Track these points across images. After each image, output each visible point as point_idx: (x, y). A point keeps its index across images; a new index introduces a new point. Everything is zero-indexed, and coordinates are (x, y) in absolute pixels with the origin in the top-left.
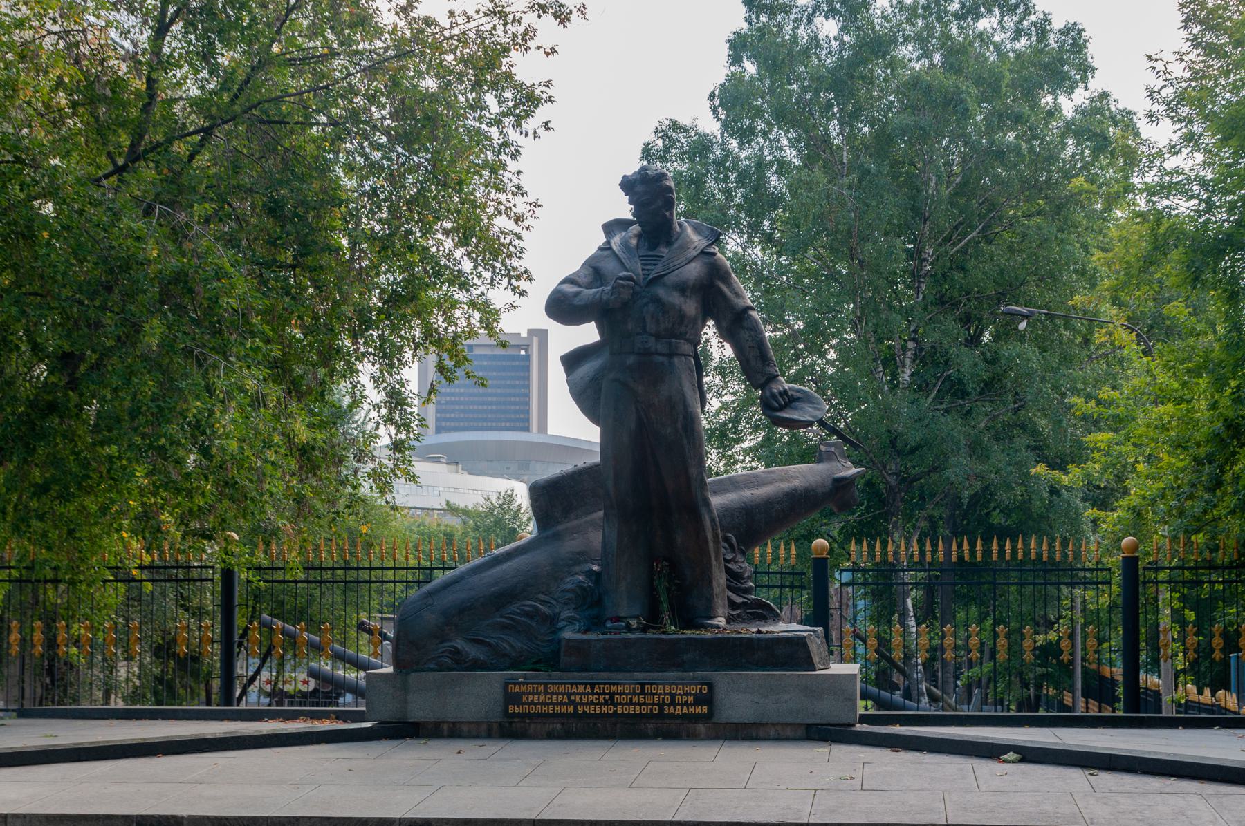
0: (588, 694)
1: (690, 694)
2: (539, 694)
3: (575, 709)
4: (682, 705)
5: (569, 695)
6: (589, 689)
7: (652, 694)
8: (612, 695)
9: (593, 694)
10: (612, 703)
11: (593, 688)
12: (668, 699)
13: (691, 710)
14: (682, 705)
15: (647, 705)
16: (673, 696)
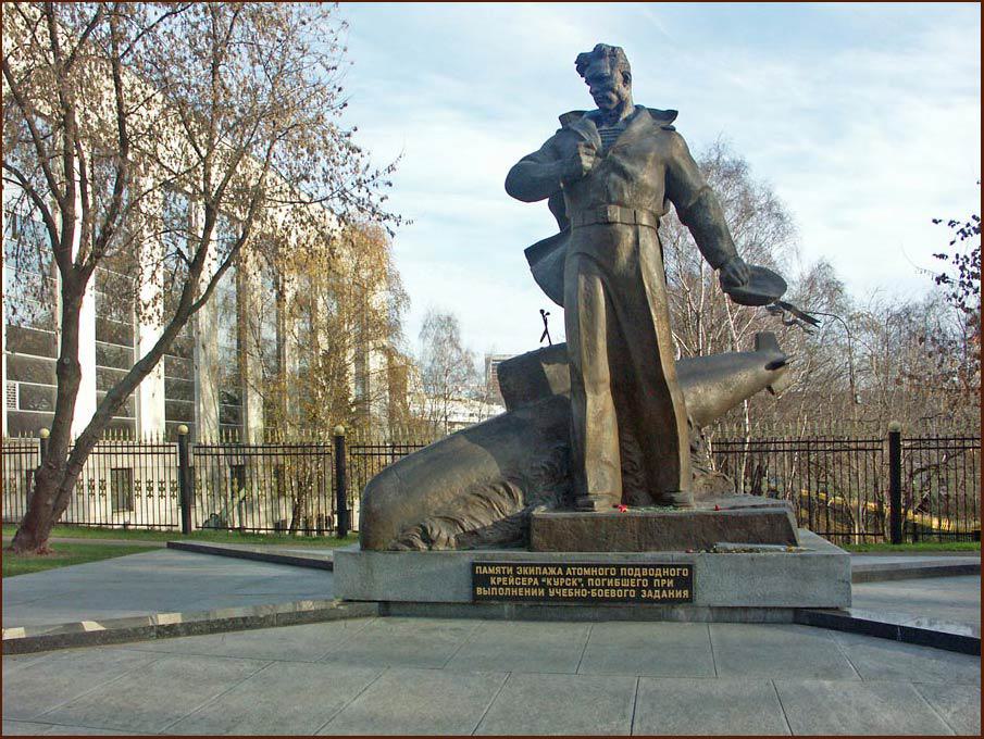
0: (559, 576)
1: (670, 577)
2: (508, 576)
3: (547, 592)
4: (661, 589)
5: (540, 577)
6: (560, 571)
7: (627, 577)
8: (585, 578)
9: (565, 577)
10: (586, 587)
11: (564, 571)
12: (645, 583)
13: (671, 594)
14: (661, 589)
15: (624, 588)
16: (651, 579)
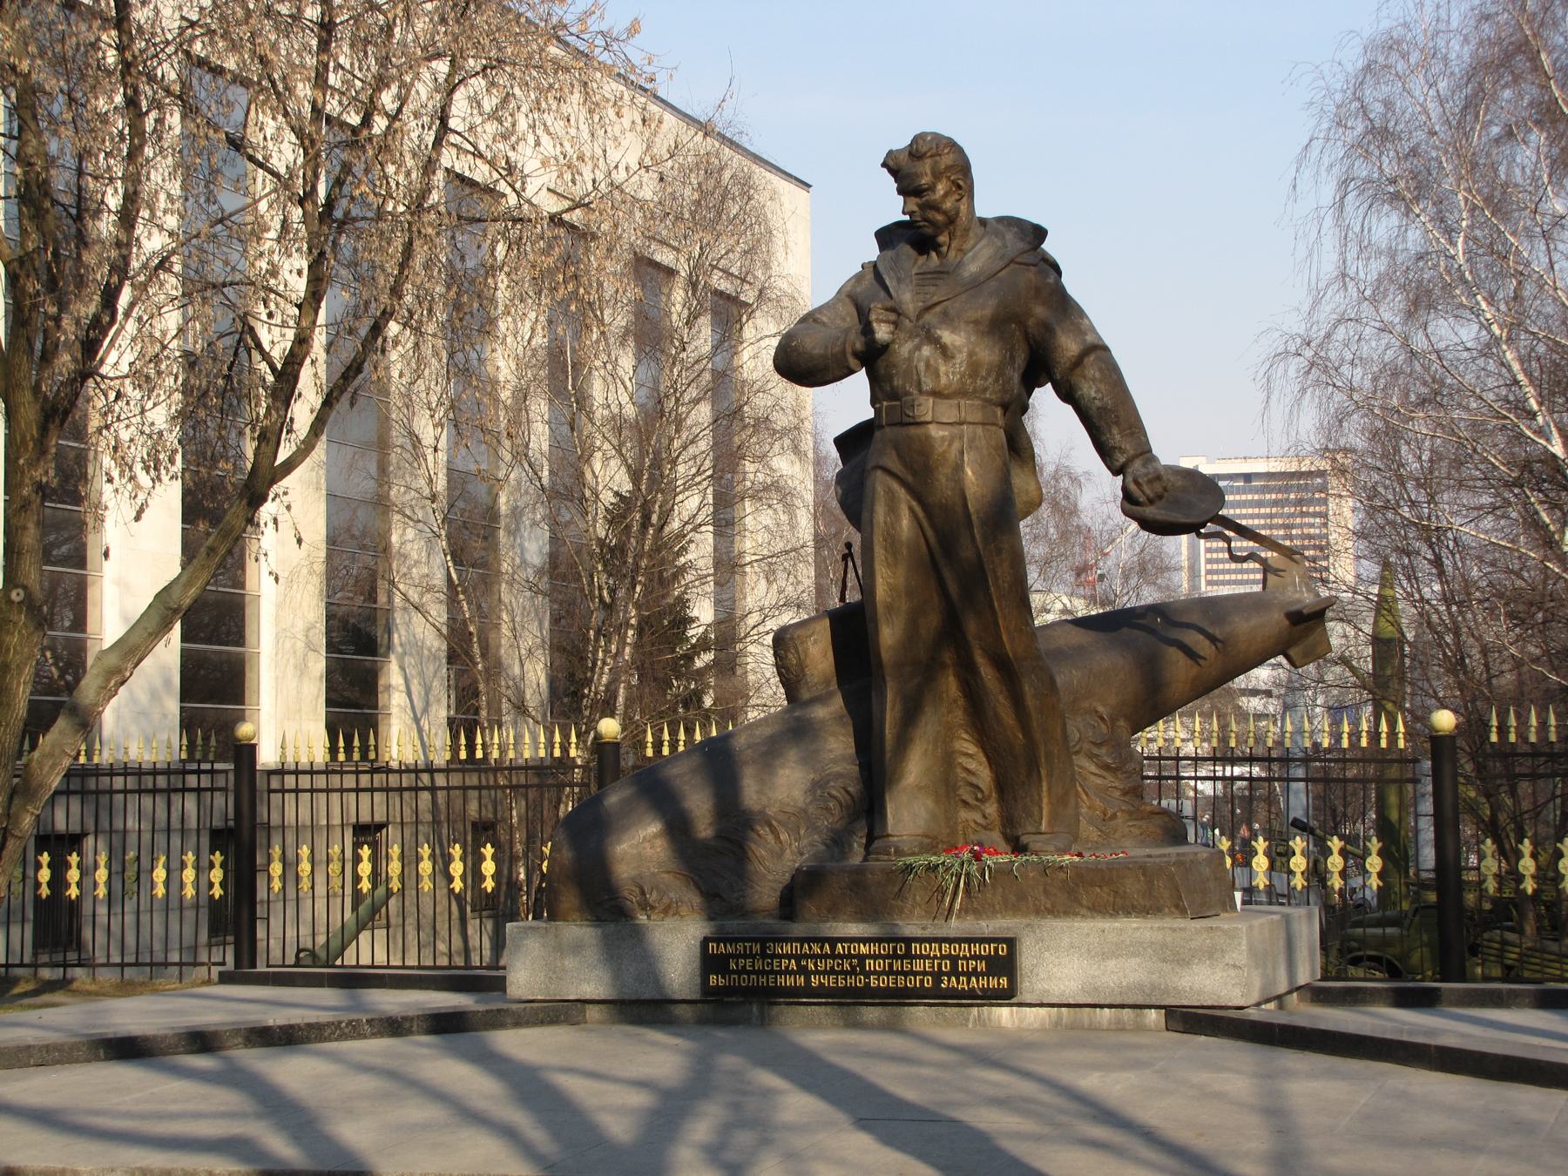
0: (826, 956)
2: (753, 956)
3: (808, 981)
4: (968, 975)
5: (798, 958)
7: (921, 957)
11: (833, 948)
12: (946, 966)
15: (915, 974)
16: (954, 960)
